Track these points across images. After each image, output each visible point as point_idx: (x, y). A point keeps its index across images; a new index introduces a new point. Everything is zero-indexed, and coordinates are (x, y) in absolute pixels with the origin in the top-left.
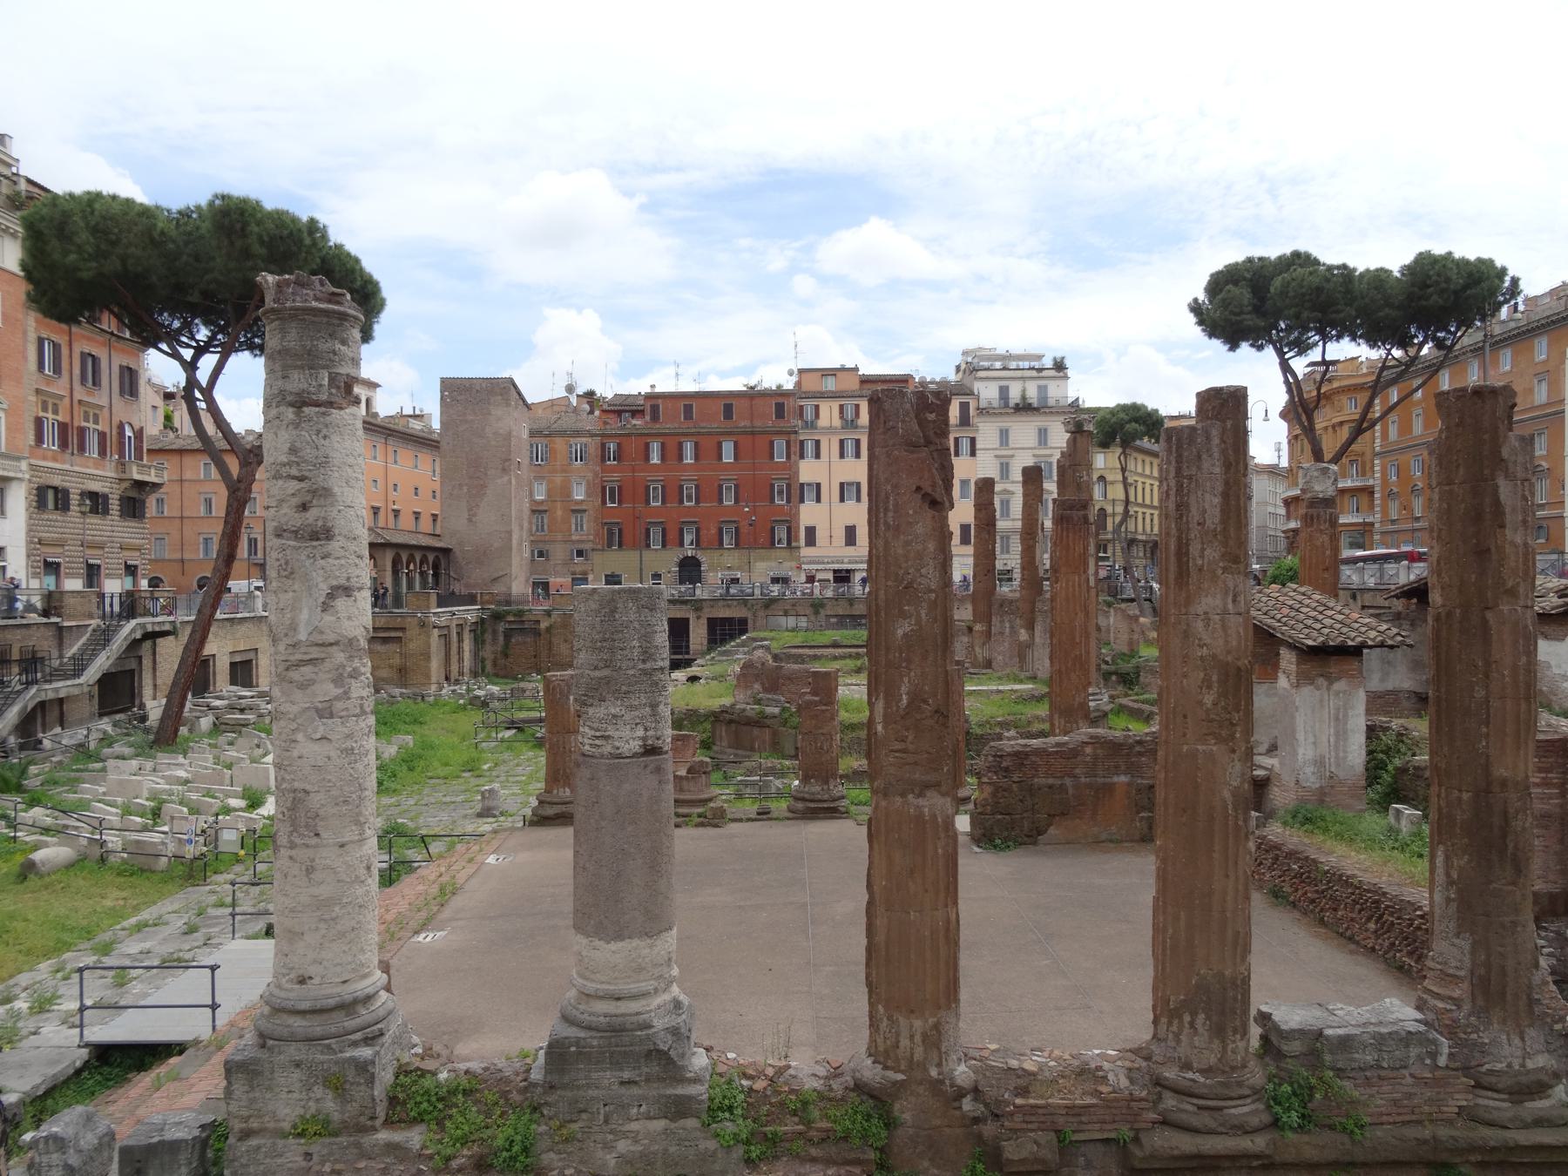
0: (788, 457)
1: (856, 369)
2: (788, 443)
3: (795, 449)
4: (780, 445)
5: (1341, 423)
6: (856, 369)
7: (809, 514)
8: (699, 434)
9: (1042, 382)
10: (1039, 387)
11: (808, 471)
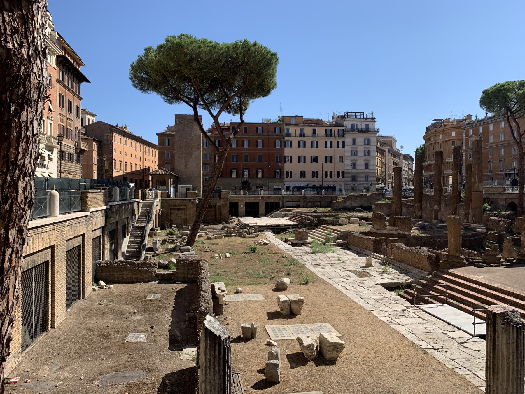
0: (281, 146)
1: (302, 116)
2: (281, 142)
3: (283, 144)
4: (278, 142)
5: (449, 140)
6: (302, 116)
7: (288, 167)
8: (249, 138)
9: (367, 123)
10: (366, 125)
11: (288, 151)
